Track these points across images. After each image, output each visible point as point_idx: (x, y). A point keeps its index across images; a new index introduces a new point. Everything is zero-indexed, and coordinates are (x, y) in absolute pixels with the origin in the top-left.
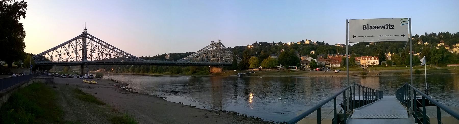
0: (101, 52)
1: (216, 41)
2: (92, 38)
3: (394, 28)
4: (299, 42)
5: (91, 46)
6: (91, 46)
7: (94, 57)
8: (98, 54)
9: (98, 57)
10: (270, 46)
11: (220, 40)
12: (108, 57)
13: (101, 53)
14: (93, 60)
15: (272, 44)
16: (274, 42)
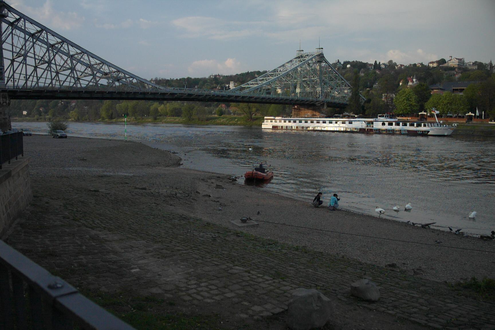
0: (46, 62)
1: (312, 50)
2: (18, 20)
3: (450, 57)
4: (433, 63)
5: (13, 45)
6: (13, 45)
7: (26, 75)
8: (33, 68)
9: (33, 75)
10: (369, 69)
11: (322, 48)
12: (62, 78)
13: (45, 66)
14: (22, 83)
15: (371, 65)
16: (376, 62)
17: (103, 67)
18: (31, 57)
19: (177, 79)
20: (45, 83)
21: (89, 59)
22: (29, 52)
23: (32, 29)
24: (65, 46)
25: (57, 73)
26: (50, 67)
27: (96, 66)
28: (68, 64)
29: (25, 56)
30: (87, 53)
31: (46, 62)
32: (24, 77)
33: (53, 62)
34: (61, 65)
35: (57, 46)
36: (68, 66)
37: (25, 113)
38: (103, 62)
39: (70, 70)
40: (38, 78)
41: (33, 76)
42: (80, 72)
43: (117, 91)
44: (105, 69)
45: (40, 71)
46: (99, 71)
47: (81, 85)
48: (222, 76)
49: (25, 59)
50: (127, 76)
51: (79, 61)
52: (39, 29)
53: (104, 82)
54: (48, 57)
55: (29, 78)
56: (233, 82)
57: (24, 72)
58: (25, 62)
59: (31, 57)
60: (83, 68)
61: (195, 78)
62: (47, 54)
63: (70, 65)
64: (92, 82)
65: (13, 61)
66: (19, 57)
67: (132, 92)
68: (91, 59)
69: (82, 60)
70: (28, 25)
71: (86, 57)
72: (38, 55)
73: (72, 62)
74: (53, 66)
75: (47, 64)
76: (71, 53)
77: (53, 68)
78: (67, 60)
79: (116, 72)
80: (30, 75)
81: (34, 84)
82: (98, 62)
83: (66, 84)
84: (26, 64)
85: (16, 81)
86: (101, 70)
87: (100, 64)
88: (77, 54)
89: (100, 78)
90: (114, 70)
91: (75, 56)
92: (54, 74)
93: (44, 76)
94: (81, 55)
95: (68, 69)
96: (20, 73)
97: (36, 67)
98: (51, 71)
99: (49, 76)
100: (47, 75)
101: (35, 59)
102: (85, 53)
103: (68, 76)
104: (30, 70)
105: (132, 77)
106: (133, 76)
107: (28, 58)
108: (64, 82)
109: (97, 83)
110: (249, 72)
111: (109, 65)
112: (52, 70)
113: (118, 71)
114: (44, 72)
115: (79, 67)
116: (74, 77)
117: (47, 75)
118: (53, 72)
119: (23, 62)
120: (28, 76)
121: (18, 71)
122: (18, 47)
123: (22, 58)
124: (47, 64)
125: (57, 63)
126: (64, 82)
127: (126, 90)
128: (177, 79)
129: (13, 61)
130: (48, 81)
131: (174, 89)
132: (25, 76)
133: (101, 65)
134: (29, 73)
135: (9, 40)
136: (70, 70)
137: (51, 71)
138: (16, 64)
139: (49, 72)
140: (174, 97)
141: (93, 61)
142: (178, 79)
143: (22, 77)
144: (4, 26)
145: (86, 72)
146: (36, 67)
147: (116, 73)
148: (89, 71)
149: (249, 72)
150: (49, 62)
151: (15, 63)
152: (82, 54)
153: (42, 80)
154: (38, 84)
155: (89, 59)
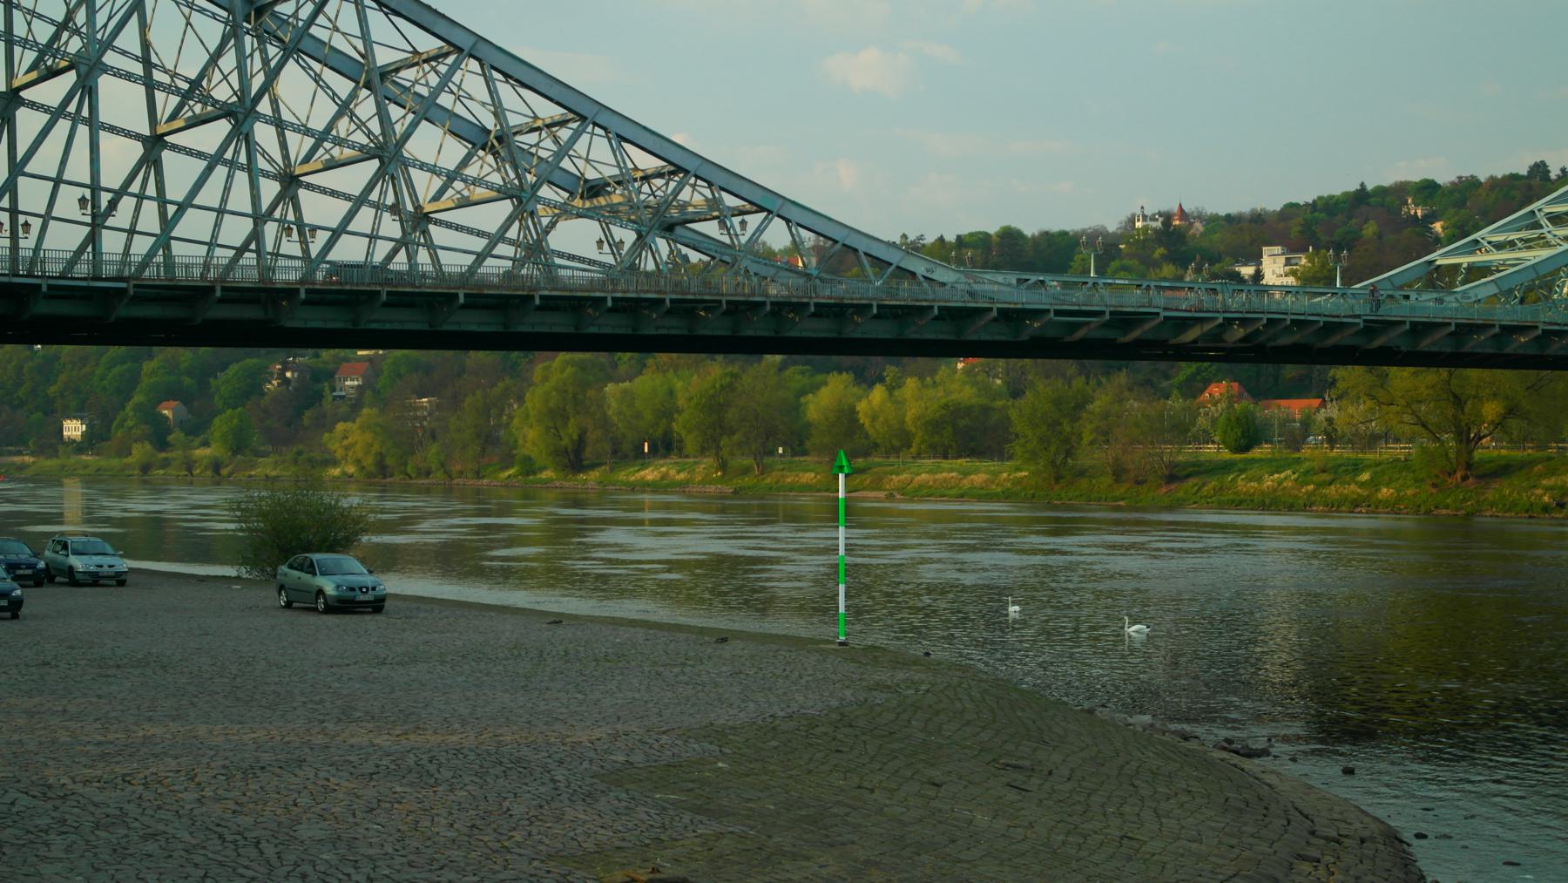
7: (95, 187)
9: (135, 187)
13: (212, 136)
14: (64, 239)
17: (581, 146)
18: (128, 76)
19: (941, 239)
20: (212, 244)
21: (492, 92)
22: (108, 45)
25: (290, 182)
26: (248, 139)
27: (532, 138)
28: (361, 125)
29: (89, 70)
30: (482, 51)
31: (225, 111)
32: (83, 201)
33: (264, 107)
34: (318, 124)
36: (360, 138)
37: (74, 429)
39: (375, 163)
40: (171, 209)
41: (141, 197)
42: (434, 170)
43: (668, 298)
46: (551, 174)
47: (435, 259)
48: (1200, 217)
49: (86, 88)
50: (730, 201)
51: (427, 110)
54: (234, 79)
55: (113, 205)
56: (1277, 249)
57: (79, 168)
58: (85, 113)
59: (128, 76)
60: (454, 152)
61: (1047, 233)
62: (228, 61)
63: (375, 126)
64: (511, 242)
66: (53, 73)
67: (763, 304)
68: (505, 91)
69: (445, 100)
72: (170, 66)
73: (382, 115)
74: (264, 134)
75: (223, 127)
76: (383, 57)
77: (264, 153)
78: (353, 95)
79: (660, 175)
80: (116, 186)
81: (141, 246)
82: (549, 111)
83: (350, 251)
84: (94, 125)
85: (27, 225)
86: (566, 164)
87: (563, 123)
88: (417, 59)
89: (565, 211)
90: (648, 162)
91: (403, 74)
92: (269, 189)
93: (210, 195)
94: (443, 69)
96: (54, 175)
97: (154, 144)
98: (250, 168)
99: (240, 198)
100: (227, 189)
101: (151, 86)
102: (471, 56)
103: (360, 201)
104: (120, 157)
105: (761, 209)
106: (766, 204)
107: (105, 83)
108: (336, 233)
109: (535, 249)
110: (1370, 187)
111: (623, 132)
112: (262, 164)
113: (678, 169)
114: (209, 170)
115: (428, 144)
116: (395, 209)
117: (227, 189)
118: (267, 175)
119: (72, 108)
120: (105, 198)
121: (45, 161)
122: (40, 17)
123: (70, 78)
124: (223, 127)
125: (286, 116)
126: (336, 233)
127: (727, 285)
128: (941, 239)
130: (236, 230)
131: (1020, 281)
132: (87, 193)
133: (564, 134)
134: (112, 177)
136: (375, 163)
137: (250, 168)
139: (241, 178)
140: (1024, 337)
141: (520, 105)
142: (950, 237)
143: (68, 201)
145: (472, 171)
146: (154, 144)
147: (659, 182)
148: (484, 166)
149: (1370, 187)
150: (240, 114)
151: (22, 114)
152: (450, 60)
153: (195, 224)
154: (167, 247)
155: (492, 92)
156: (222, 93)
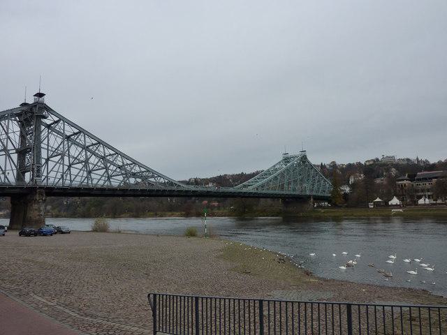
13: (80, 166)
23: (69, 131)
24: (101, 148)
29: (63, 155)
31: (82, 162)
35: (91, 148)
38: (135, 163)
44: (137, 169)
45: (74, 171)
49: (62, 158)
52: (76, 131)
53: (132, 181)
57: (61, 170)
65: (47, 160)
70: (67, 128)
71: (119, 158)
83: (101, 182)
95: (103, 168)
97: (70, 166)
103: (102, 176)
104: (66, 168)
111: (140, 166)
129: (47, 160)
133: (132, 166)
135: (46, 141)
138: (51, 164)
144: (43, 127)
146: (70, 166)
156: (82, 159)
